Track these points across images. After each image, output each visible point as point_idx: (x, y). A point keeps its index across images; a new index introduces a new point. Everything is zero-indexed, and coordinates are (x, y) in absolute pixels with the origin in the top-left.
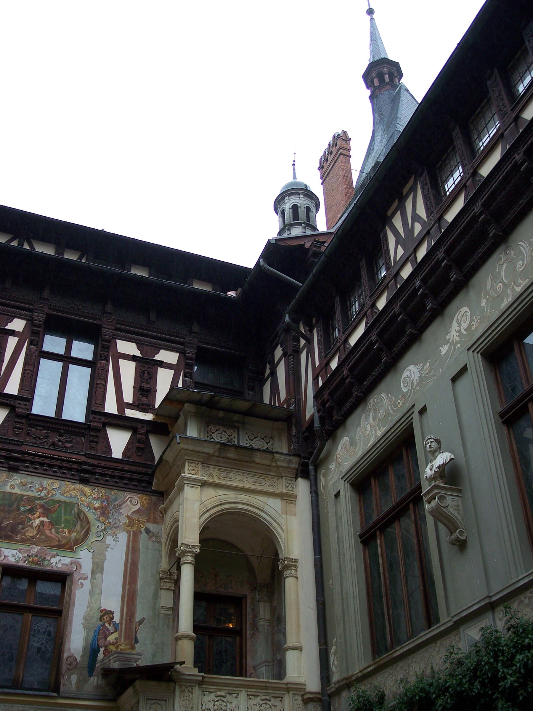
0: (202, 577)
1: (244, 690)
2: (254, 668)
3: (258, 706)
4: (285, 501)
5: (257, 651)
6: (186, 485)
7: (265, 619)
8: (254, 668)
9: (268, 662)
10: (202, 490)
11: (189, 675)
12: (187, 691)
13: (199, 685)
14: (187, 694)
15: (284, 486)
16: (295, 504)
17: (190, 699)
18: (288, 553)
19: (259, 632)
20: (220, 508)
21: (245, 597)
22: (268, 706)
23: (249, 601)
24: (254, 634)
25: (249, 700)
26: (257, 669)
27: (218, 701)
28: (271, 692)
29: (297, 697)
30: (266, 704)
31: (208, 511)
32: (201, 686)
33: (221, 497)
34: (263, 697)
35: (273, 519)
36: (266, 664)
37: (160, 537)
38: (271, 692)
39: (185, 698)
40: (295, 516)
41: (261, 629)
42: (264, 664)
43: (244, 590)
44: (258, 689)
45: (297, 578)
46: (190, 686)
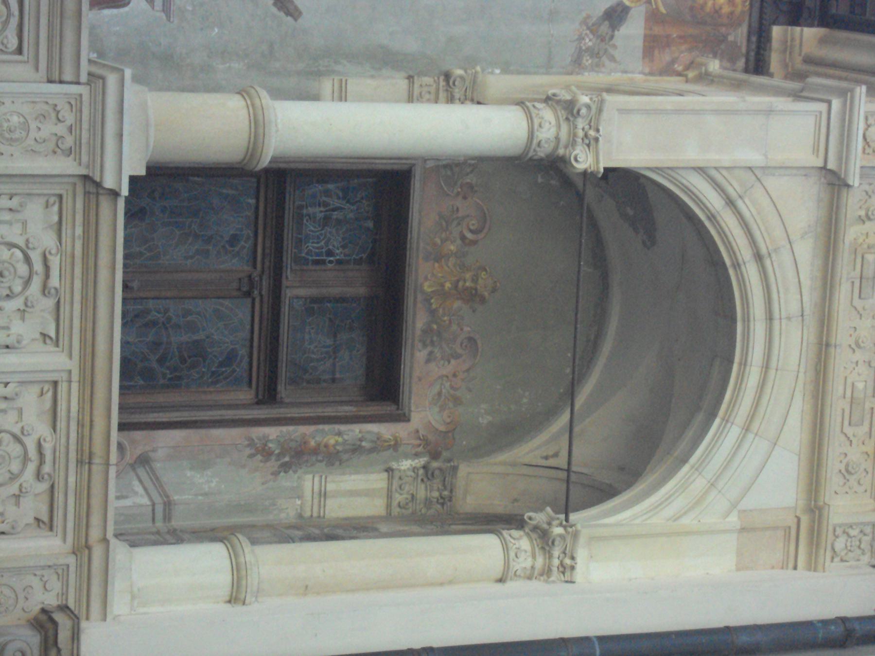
0: (463, 238)
1: (73, 365)
2: (144, 461)
3: (17, 430)
4: (792, 523)
5: (210, 468)
6: (823, 107)
7: (323, 495)
8: (144, 461)
9: (167, 517)
10: (805, 171)
11: (120, 136)
12: (61, 129)
13: (86, 178)
14: (49, 129)
15: (851, 520)
16: (782, 568)
17: (30, 142)
18: (592, 539)
19: (275, 474)
20: (745, 253)
21: (404, 418)
22: (15, 467)
23: (385, 430)
24: (267, 454)
25: (36, 389)
26: (141, 472)
27: (27, 260)
28: (72, 479)
29: (55, 585)
30: (25, 459)
31: (730, 203)
32: (80, 190)
33: (786, 257)
34: (48, 447)
35: (752, 417)
36: (159, 509)
37: (597, 67)
38: (72, 479)
39: (33, 125)
40: (738, 569)
41: (287, 481)
42: (158, 499)
43: (424, 412)
44: (80, 424)
45: (501, 580)
46: (78, 143)
